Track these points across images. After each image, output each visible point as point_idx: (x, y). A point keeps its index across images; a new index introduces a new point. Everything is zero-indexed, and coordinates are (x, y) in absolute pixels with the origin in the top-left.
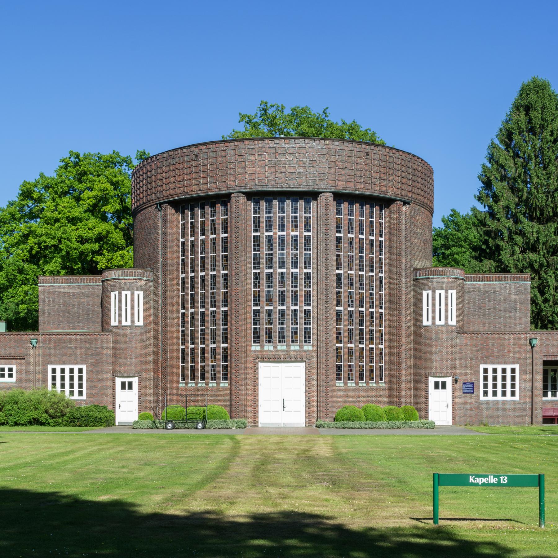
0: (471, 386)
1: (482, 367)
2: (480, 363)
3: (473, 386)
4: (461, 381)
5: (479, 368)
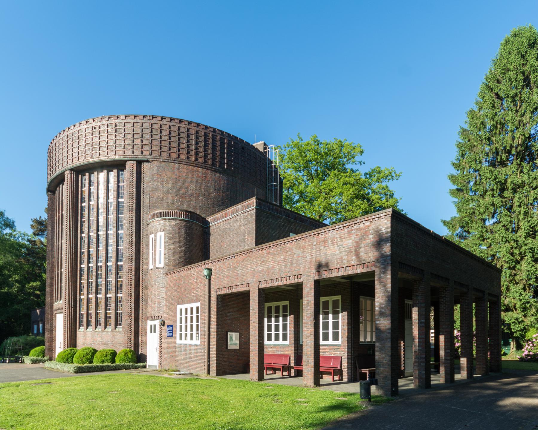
0: (171, 329)
1: (179, 307)
2: (176, 304)
3: (173, 328)
4: (166, 324)
5: (176, 309)
